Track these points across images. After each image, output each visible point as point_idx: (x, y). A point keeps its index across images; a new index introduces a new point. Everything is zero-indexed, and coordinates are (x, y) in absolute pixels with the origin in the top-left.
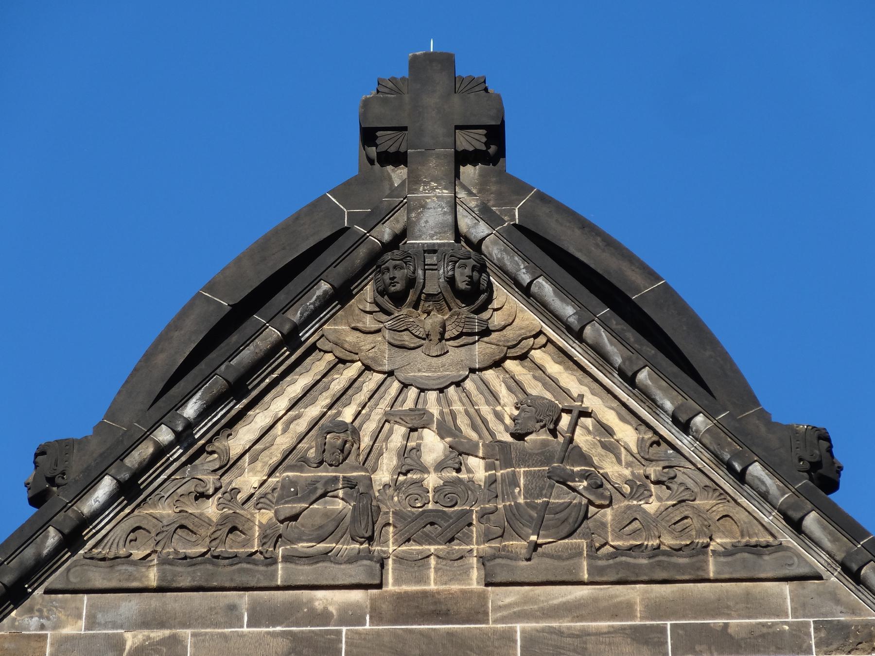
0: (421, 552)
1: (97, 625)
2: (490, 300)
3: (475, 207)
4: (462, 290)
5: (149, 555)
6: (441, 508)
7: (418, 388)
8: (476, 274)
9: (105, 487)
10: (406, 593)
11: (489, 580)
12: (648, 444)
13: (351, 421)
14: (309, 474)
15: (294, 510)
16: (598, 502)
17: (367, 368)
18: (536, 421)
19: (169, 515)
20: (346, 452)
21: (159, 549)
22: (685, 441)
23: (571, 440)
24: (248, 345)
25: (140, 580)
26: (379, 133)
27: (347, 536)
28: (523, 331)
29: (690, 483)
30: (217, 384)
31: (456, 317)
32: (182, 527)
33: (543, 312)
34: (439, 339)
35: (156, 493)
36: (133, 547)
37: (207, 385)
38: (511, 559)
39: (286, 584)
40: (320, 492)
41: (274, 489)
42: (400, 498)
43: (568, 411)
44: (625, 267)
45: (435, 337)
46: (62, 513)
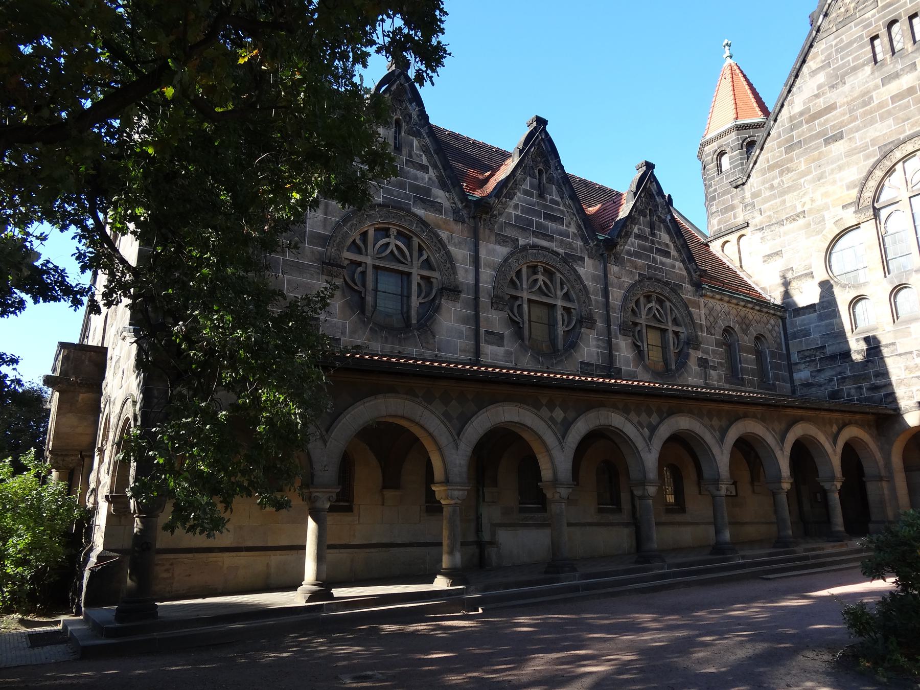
9: (821, 17)
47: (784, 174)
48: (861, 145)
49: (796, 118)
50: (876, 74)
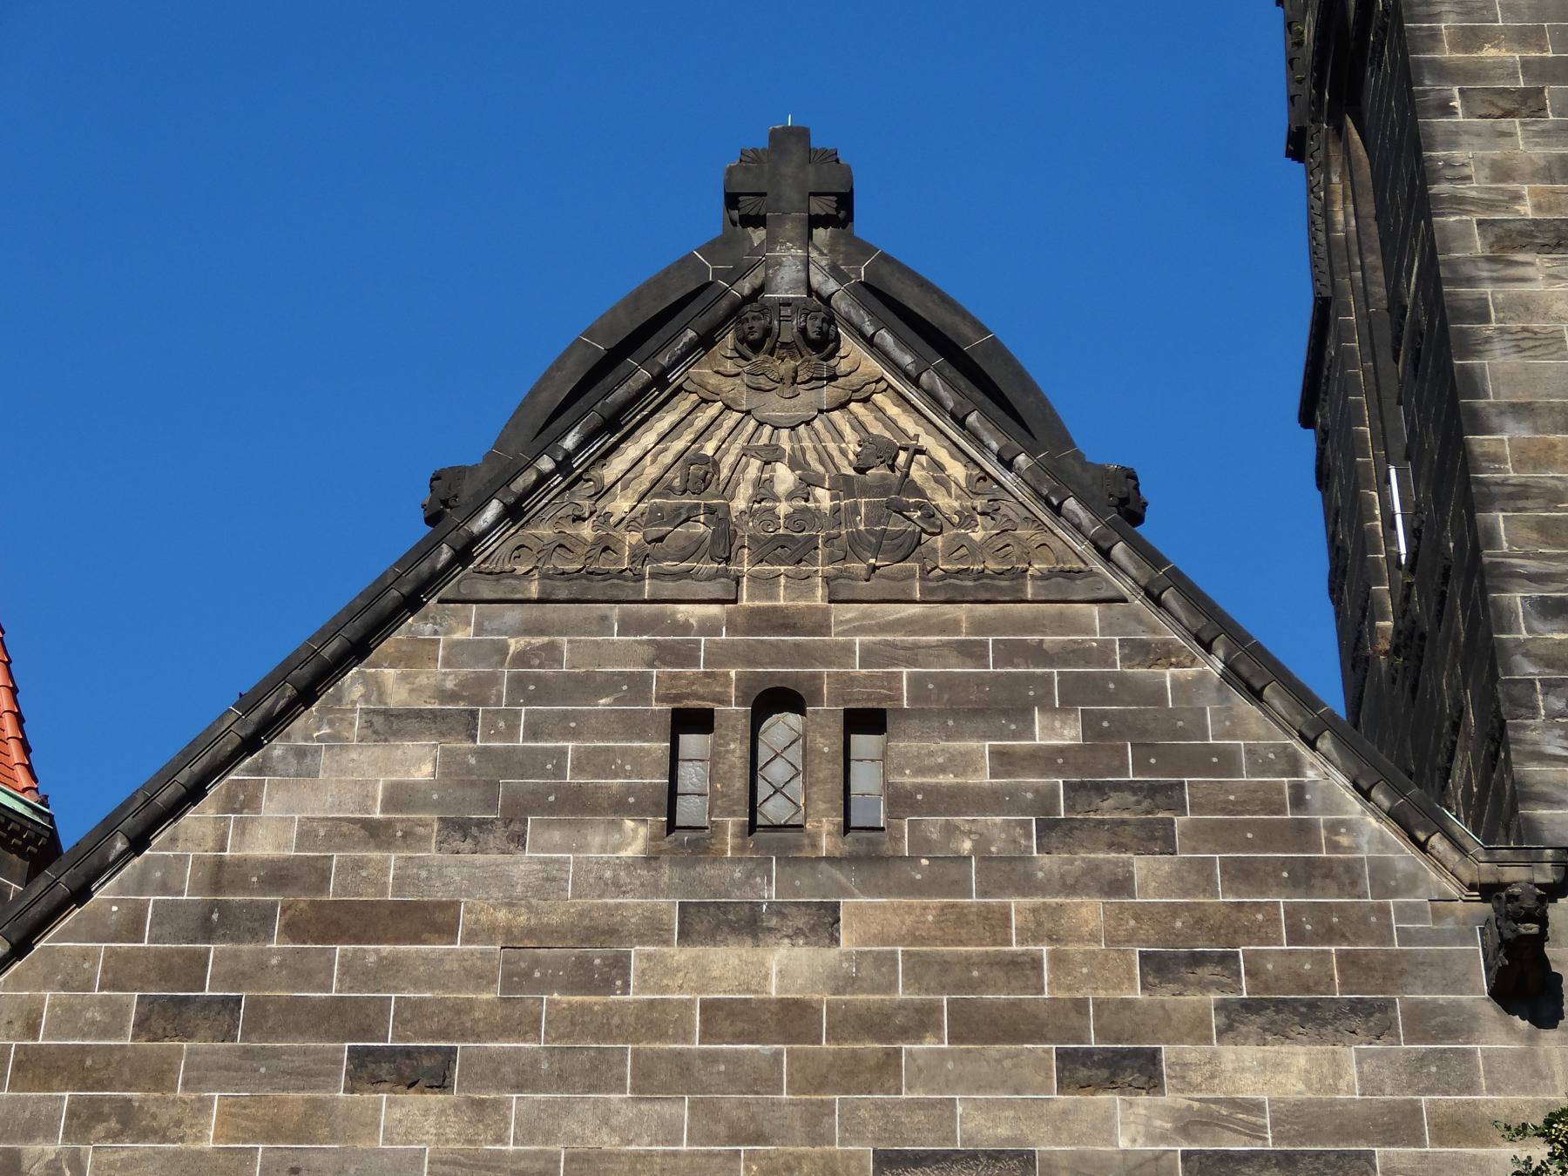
0: (773, 571)
2: (837, 349)
5: (531, 570)
6: (791, 533)
9: (493, 509)
10: (758, 607)
12: (975, 479)
14: (673, 501)
16: (930, 530)
17: (728, 407)
19: (549, 535)
20: (707, 483)
21: (540, 565)
22: (1009, 478)
23: (907, 475)
25: (523, 593)
26: (741, 198)
27: (707, 557)
29: (1012, 515)
30: (593, 419)
32: (561, 546)
35: (539, 514)
36: (517, 564)
40: (684, 517)
41: (642, 514)
43: (905, 449)
44: (957, 320)
46: (454, 532)
47: (100, 1129)
48: (520, 1156)
49: (241, 884)
50: (667, 873)
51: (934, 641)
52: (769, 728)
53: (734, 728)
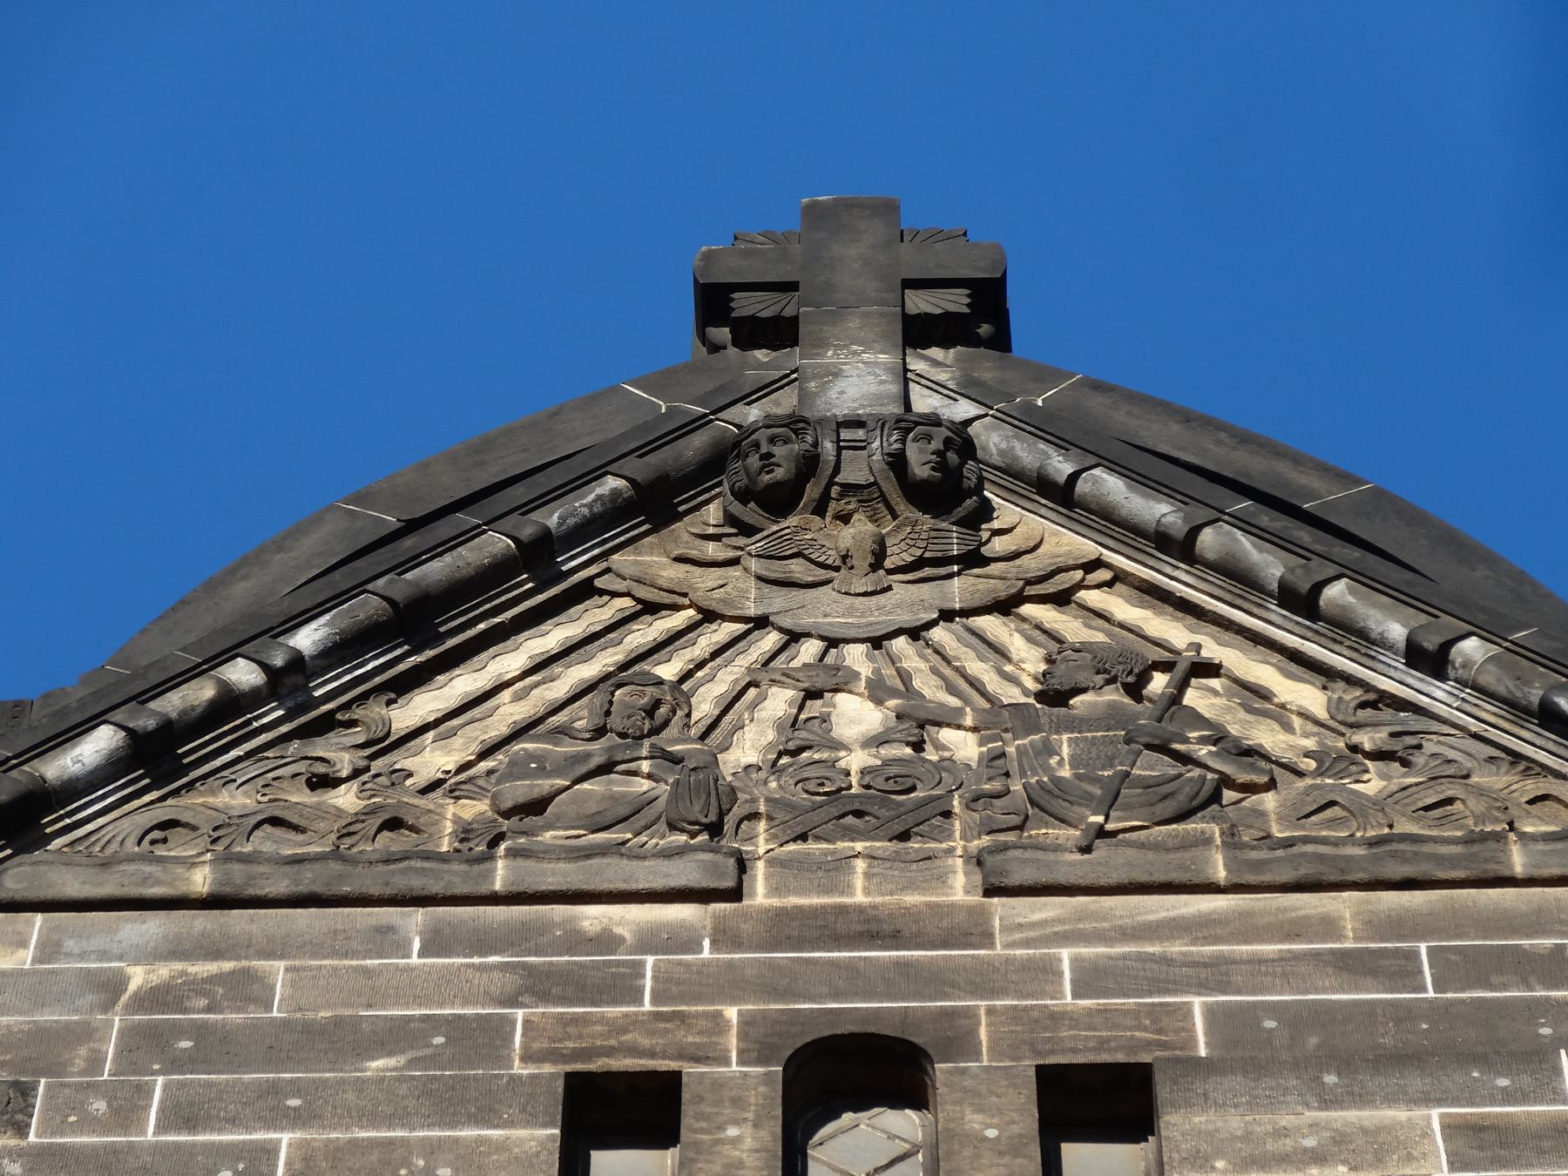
1: (62, 957)
3: (948, 380)
4: (924, 482)
7: (822, 638)
8: (952, 457)
9: (98, 745)
11: (993, 880)
13: (675, 679)
15: (536, 790)
16: (1243, 777)
18: (1094, 671)
22: (1440, 694)
24: (440, 554)
25: (171, 884)
26: (735, 295)
27: (662, 826)
28: (1060, 559)
31: (909, 529)
33: (1103, 529)
34: (871, 565)
37: (345, 606)
38: (1044, 850)
39: (514, 889)
42: (782, 782)
43: (1166, 667)
45: (862, 562)
51: (1274, 951)
52: (832, 1136)
53: (737, 1102)
